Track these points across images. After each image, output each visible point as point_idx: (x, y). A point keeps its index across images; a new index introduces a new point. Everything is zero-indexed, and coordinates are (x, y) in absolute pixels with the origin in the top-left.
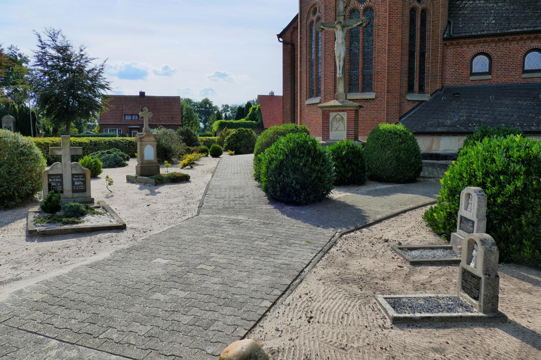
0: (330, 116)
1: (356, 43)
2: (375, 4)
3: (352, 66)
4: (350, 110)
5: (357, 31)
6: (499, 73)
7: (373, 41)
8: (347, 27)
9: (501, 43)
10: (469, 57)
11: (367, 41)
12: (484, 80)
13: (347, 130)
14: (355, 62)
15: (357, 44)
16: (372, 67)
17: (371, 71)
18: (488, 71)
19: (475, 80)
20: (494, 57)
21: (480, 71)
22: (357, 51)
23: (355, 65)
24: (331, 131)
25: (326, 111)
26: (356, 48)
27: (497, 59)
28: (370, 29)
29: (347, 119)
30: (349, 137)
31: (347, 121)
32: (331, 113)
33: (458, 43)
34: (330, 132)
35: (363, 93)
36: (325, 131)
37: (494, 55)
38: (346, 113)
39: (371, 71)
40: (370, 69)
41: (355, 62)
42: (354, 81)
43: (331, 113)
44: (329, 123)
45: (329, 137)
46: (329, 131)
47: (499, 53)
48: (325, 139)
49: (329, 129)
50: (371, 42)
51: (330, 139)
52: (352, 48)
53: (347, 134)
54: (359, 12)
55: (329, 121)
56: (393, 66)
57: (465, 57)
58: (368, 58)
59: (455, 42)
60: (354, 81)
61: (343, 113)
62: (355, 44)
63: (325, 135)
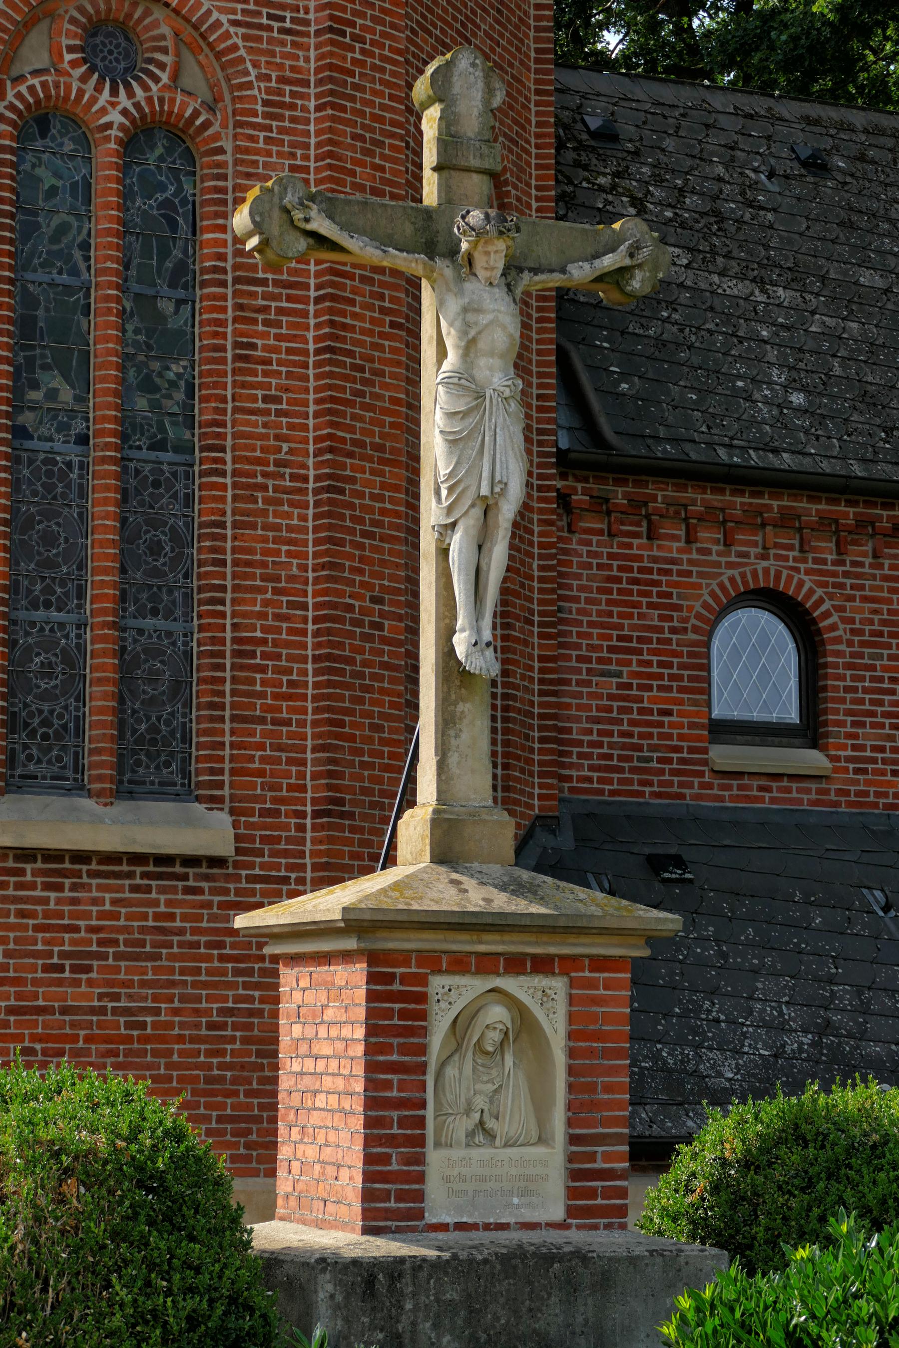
0: (434, 1008)
1: (56, 381)
2: (212, 110)
3: (28, 567)
4: (600, 963)
5: (68, 289)
6: (868, 736)
7: (191, 394)
8: (535, 271)
9: (869, 548)
10: (698, 607)
11: (148, 386)
12: (793, 777)
13: (573, 1140)
14: (49, 539)
15: (67, 395)
16: (188, 597)
17: (177, 627)
18: (793, 716)
19: (739, 775)
20: (833, 627)
21: (756, 715)
22: (73, 453)
23: (50, 564)
24: (437, 1145)
25: (404, 958)
26: (63, 428)
27: (850, 643)
28: (165, 290)
29: (571, 1035)
30: (592, 1194)
31: (572, 1053)
32: (438, 983)
33: (637, 505)
34: (435, 1157)
35: (121, 808)
36: (392, 1141)
37: (835, 618)
38: (557, 985)
39: (177, 627)
40: (169, 615)
41: (49, 539)
42: (45, 696)
43: (438, 983)
44: (422, 1068)
45: (419, 1196)
46: (421, 1141)
47: (859, 611)
48: (388, 1214)
49: (421, 1122)
50: (180, 396)
51: (431, 1218)
52: (27, 418)
53: (575, 1175)
54: (85, 143)
55: (422, 1050)
56: (364, 611)
57: (677, 608)
58: (155, 524)
59: (619, 495)
60: (45, 696)
61: (540, 981)
62: (52, 394)
63: (384, 1177)
